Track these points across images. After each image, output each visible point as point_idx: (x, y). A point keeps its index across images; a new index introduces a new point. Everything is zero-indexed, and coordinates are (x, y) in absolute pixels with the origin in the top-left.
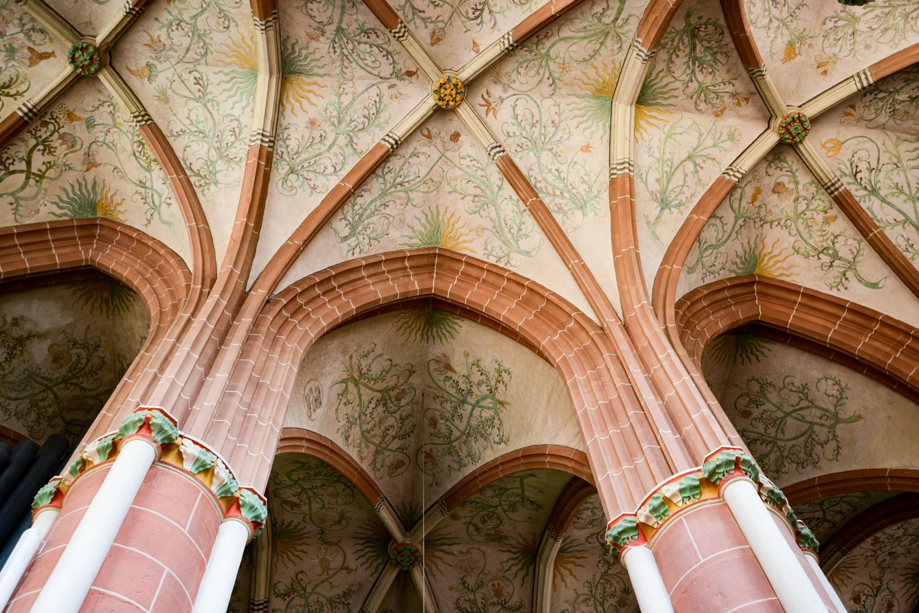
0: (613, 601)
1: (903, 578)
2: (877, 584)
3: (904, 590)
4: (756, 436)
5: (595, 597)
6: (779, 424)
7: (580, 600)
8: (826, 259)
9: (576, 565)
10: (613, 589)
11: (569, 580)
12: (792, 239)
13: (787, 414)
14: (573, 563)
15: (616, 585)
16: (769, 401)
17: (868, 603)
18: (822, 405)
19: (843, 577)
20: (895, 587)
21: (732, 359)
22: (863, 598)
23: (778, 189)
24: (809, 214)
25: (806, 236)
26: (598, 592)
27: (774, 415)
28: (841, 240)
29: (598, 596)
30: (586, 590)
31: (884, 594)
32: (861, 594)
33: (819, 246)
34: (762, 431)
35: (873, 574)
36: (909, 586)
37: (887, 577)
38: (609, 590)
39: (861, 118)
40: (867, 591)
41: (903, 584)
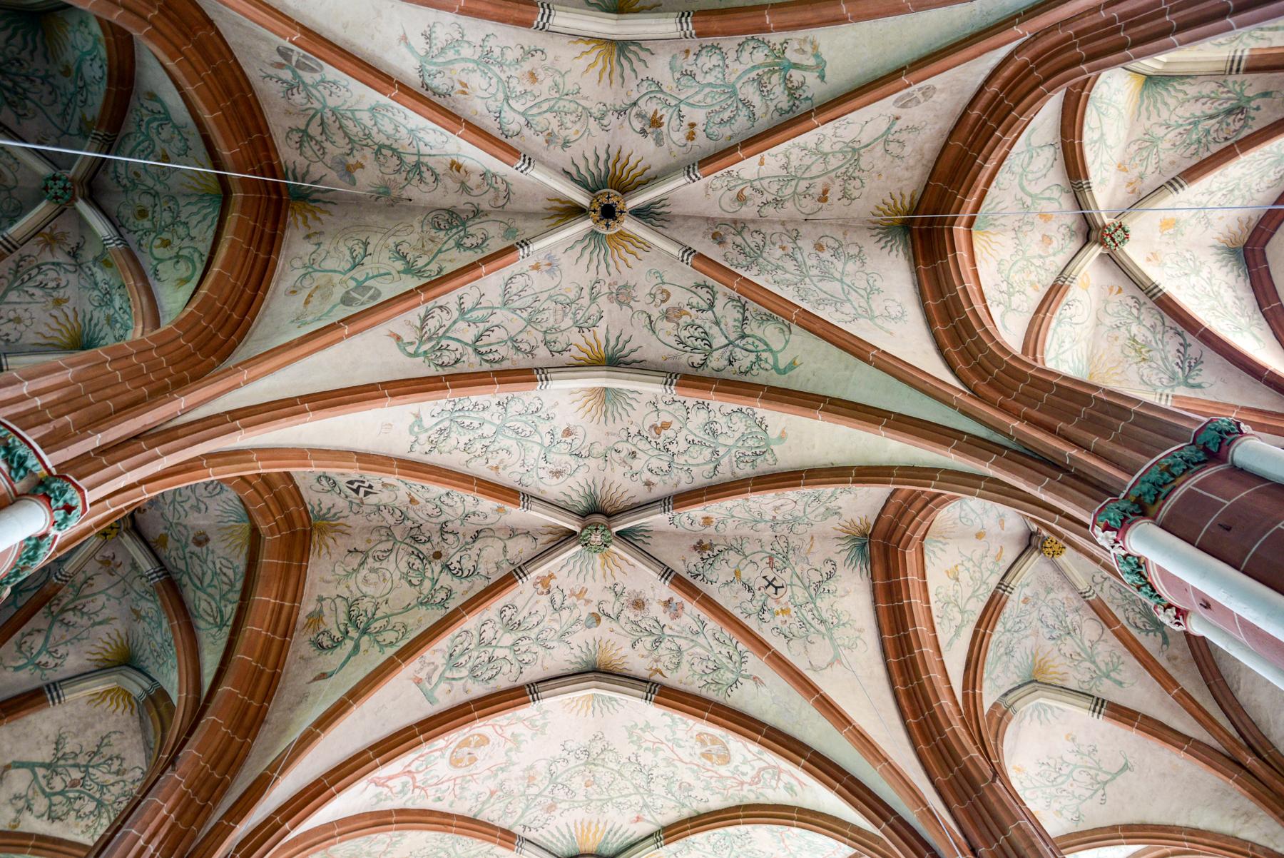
0: (554, 126)
1: (590, 482)
2: (584, 453)
4: (800, 259)
5: (560, 99)
6: (825, 275)
7: (557, 78)
8: (1004, 287)
9: (601, 73)
10: (569, 125)
11: (583, 63)
12: (1008, 258)
13: (841, 281)
14: (604, 68)
15: (574, 129)
16: (845, 264)
17: (563, 446)
18: (874, 307)
19: (593, 411)
21: (872, 225)
22: (569, 440)
23: (1047, 239)
24: (1033, 268)
25: (1015, 268)
26: (566, 103)
27: (832, 271)
28: (1023, 297)
29: (561, 103)
30: (570, 87)
33: (1011, 280)
34: (809, 263)
36: (581, 490)
37: (592, 462)
38: (568, 119)
39: (1106, 302)
40: (577, 443)
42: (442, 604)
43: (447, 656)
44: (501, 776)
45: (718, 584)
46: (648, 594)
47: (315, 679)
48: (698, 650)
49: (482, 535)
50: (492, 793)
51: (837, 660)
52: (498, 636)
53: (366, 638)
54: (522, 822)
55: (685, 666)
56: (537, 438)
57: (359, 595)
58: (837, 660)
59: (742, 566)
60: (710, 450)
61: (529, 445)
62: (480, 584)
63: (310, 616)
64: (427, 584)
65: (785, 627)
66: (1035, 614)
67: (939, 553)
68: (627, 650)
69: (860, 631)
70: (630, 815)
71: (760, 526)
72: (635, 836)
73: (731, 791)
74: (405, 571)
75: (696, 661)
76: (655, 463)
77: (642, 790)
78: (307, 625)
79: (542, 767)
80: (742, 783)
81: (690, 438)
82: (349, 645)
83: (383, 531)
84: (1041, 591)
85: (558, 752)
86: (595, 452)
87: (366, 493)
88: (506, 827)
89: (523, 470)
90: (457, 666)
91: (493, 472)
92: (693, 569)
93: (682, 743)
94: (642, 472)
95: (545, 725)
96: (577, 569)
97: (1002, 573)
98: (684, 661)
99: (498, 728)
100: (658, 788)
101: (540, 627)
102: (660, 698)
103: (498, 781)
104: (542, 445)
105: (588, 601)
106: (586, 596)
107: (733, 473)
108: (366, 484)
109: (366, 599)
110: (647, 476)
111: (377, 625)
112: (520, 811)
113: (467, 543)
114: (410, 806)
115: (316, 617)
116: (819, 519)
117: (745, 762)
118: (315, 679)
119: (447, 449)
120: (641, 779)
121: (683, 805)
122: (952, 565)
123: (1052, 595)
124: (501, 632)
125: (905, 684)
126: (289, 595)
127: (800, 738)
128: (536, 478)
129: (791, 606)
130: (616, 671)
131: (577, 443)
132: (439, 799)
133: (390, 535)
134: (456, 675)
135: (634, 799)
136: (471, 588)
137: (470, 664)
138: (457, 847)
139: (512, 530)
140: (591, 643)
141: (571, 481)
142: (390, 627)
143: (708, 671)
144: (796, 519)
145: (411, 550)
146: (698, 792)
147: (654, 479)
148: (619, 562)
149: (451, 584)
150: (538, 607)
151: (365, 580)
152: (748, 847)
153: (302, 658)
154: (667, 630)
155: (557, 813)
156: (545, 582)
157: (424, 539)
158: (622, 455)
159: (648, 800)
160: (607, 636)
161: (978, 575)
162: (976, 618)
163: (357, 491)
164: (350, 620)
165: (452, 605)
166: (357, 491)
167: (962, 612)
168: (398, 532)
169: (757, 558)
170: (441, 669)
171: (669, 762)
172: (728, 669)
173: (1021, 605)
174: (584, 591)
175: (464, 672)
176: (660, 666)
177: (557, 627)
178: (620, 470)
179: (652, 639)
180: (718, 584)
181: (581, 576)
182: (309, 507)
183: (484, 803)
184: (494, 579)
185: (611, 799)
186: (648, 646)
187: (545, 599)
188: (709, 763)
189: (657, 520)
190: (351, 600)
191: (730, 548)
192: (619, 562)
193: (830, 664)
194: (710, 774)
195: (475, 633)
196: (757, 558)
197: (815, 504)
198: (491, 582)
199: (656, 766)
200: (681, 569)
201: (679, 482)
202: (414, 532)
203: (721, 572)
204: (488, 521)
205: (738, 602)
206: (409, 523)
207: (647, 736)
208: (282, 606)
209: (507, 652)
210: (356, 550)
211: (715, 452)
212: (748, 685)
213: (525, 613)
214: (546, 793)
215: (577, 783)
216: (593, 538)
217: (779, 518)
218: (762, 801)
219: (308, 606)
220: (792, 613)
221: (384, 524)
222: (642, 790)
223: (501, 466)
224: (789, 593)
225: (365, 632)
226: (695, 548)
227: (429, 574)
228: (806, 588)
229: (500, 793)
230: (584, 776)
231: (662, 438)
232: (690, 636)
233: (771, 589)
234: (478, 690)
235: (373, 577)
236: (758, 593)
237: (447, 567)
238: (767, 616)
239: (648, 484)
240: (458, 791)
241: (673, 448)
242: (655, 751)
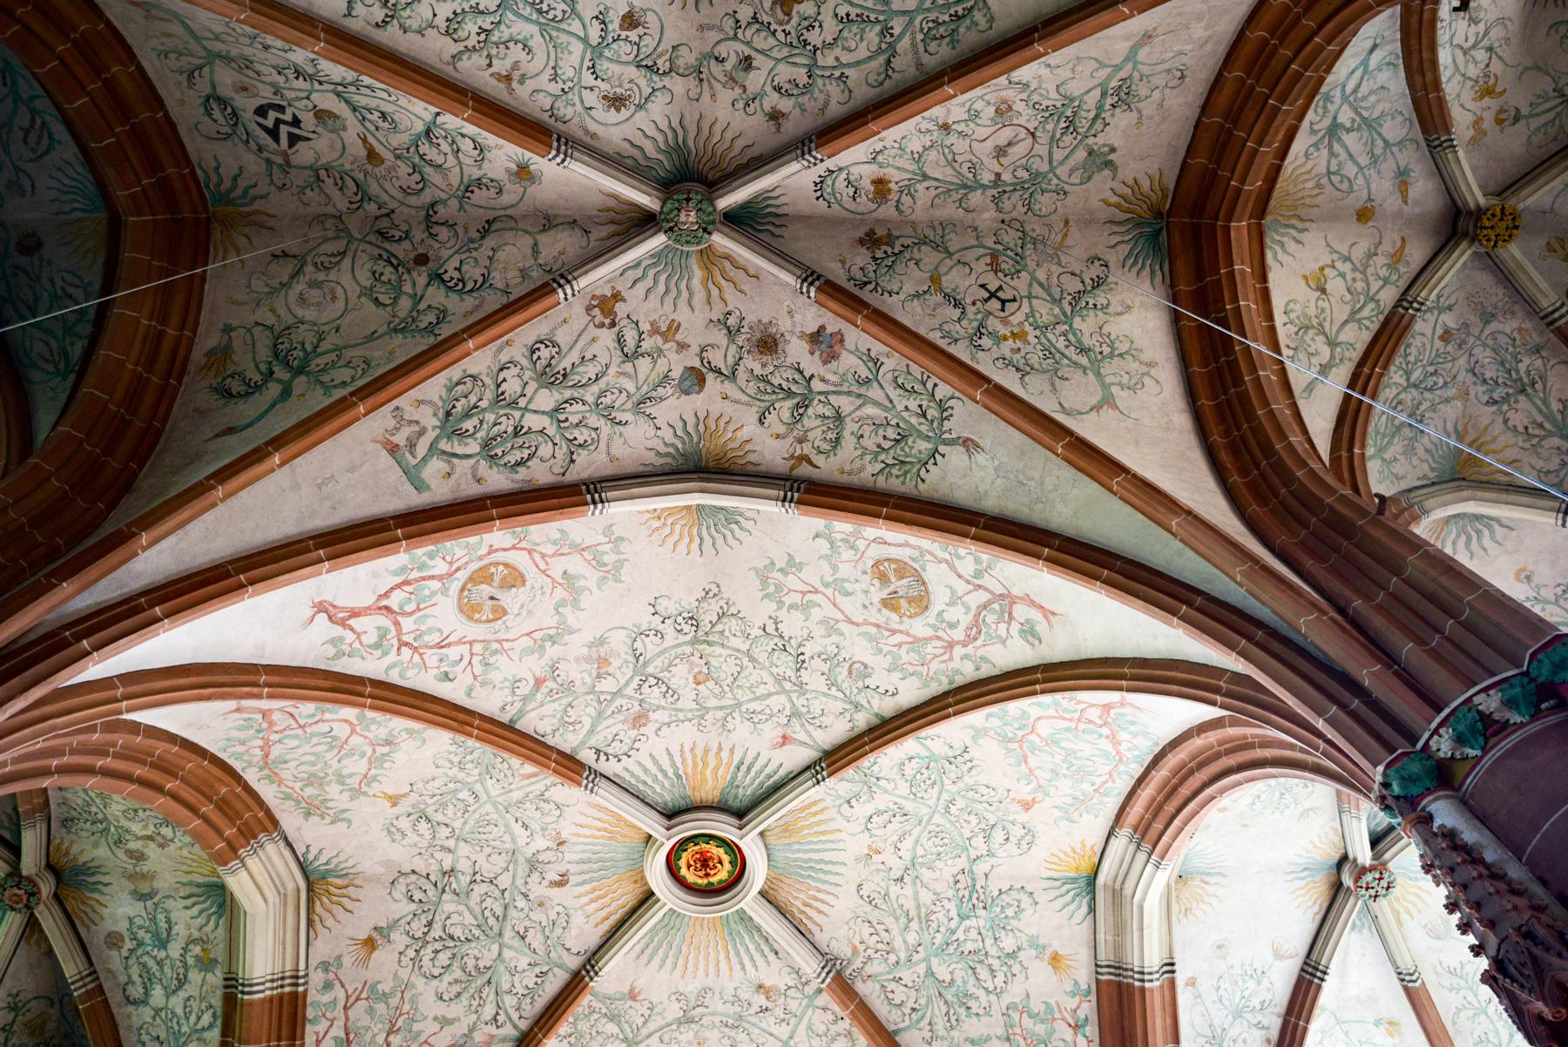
1: (676, 124)
2: (663, 64)
3: (652, 132)
20: (658, 109)
22: (633, 35)
31: (643, 83)
32: (640, 30)
35: (683, 51)
36: (660, 138)
37: (678, 85)
40: (649, 43)
41: (664, 125)
42: (430, 329)
43: (441, 414)
44: (552, 652)
45: (902, 296)
46: (784, 324)
47: (217, 436)
48: (870, 410)
49: (494, 228)
50: (539, 683)
51: (1108, 401)
52: (529, 391)
53: (302, 379)
54: (593, 742)
55: (848, 442)
56: (575, 26)
57: (291, 321)
58: (1108, 401)
59: (942, 270)
60: (878, 28)
61: (563, 38)
62: (493, 302)
63: (211, 353)
64: (405, 304)
65: (1018, 356)
66: (1462, 362)
67: (1292, 246)
68: (750, 429)
69: (1150, 365)
70: (771, 732)
71: (976, 198)
72: (782, 772)
73: (934, 666)
74: (368, 284)
75: (867, 430)
76: (785, 73)
77: (788, 686)
78: (207, 367)
79: (619, 642)
80: (951, 645)
81: (842, 11)
82: (274, 389)
83: (329, 223)
84: (1474, 319)
85: (646, 619)
86: (680, 62)
87: (294, 139)
88: (566, 748)
89: (554, 88)
90: (462, 435)
91: (502, 86)
92: (859, 275)
93: (849, 587)
94: (761, 95)
95: (619, 565)
96: (661, 288)
97: (1403, 284)
98: (846, 433)
99: (537, 557)
100: (813, 678)
101: (602, 383)
102: (808, 497)
103: (546, 660)
104: (585, 40)
105: (682, 346)
106: (678, 337)
107: (919, 65)
108: (288, 117)
109: (303, 327)
110: (772, 100)
111: (321, 361)
113: (472, 241)
114: (394, 678)
115: (222, 354)
116: (1075, 179)
117: (954, 600)
118: (217, 436)
119: (415, 26)
120: (785, 665)
121: (857, 707)
122: (1316, 266)
123: (1494, 326)
124: (532, 386)
125: (1227, 433)
126: (175, 318)
127: (1041, 524)
128: (579, 108)
129: (1028, 328)
130: (736, 468)
131: (649, 43)
132: (446, 677)
133: (342, 230)
134: (460, 450)
136: (478, 307)
137: (481, 434)
138: (489, 783)
139: (547, 218)
140: (691, 421)
141: (641, 119)
142: (341, 363)
143: (887, 445)
144: (1036, 177)
145: (377, 252)
146: (880, 679)
147: (785, 105)
148: (732, 272)
149: (445, 302)
150: (595, 349)
151: (302, 299)
152: (968, 780)
153: (197, 410)
154: (817, 385)
155: (649, 730)
156: (605, 307)
157: (397, 234)
158: (729, 65)
159: (800, 702)
160: (717, 407)
161: (1360, 286)
162: (1356, 355)
163: (274, 133)
164: (276, 355)
165: (445, 331)
166: (274, 133)
167: (1332, 344)
168: (353, 223)
169: (970, 256)
170: (431, 435)
172: (920, 435)
173: (1438, 344)
174: (673, 327)
175: (473, 447)
176: (807, 449)
177: (630, 386)
178: (726, 95)
179: (790, 403)
180: (902, 296)
181: (669, 300)
182: (200, 173)
183: (525, 699)
184: (516, 293)
185: (739, 705)
186: (786, 415)
187: (607, 337)
188: (894, 617)
189: (792, 181)
190: (277, 329)
191: (924, 241)
192: (732, 272)
193: (1096, 408)
194: (898, 638)
195: (488, 381)
196: (970, 256)
197: (1068, 139)
198: (512, 298)
199: (810, 637)
200: (838, 274)
201: (826, 104)
202: (384, 223)
203: (909, 279)
204: (506, 199)
205: (936, 323)
206: (371, 208)
207: (792, 582)
208: (161, 335)
209: (545, 421)
210: (285, 254)
211: (886, 31)
212: (955, 457)
213: (574, 357)
214: (629, 691)
215: (680, 676)
216: (683, 218)
217: (1006, 177)
218: (986, 671)
219: (208, 340)
220: (1031, 338)
221: (330, 209)
222: (788, 686)
223: (516, 75)
224: (1025, 309)
225: (300, 371)
226: (861, 242)
227: (408, 288)
228: (1057, 301)
229: (551, 684)
230: (692, 664)
231: (794, 21)
232: (855, 388)
233: (995, 305)
234: (498, 480)
235: (314, 295)
236: (971, 310)
237: (437, 277)
238: (986, 342)
239: (775, 116)
240: (478, 669)
241: (814, 37)
242: (805, 608)
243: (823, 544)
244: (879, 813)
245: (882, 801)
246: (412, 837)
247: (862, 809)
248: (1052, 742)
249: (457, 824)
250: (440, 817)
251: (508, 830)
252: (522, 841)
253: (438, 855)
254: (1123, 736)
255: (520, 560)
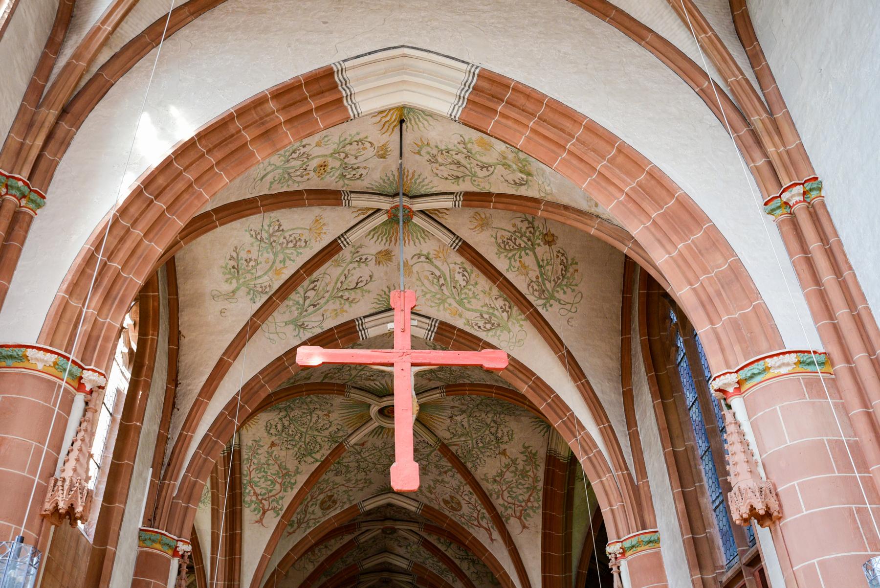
44: (440, 478)
50: (446, 472)
70: (368, 445)
100: (353, 465)
112: (433, 455)
121: (338, 463)
135: (367, 454)
152: (296, 449)
171: (349, 480)
207: (361, 486)
242: (357, 481)
243: (352, 498)
244: (327, 429)
245: (326, 433)
246: (505, 431)
247: (333, 428)
248: (273, 482)
249: (487, 432)
250: (492, 437)
251: (470, 426)
252: (466, 420)
253: (499, 420)
254: (254, 498)
255: (442, 504)
